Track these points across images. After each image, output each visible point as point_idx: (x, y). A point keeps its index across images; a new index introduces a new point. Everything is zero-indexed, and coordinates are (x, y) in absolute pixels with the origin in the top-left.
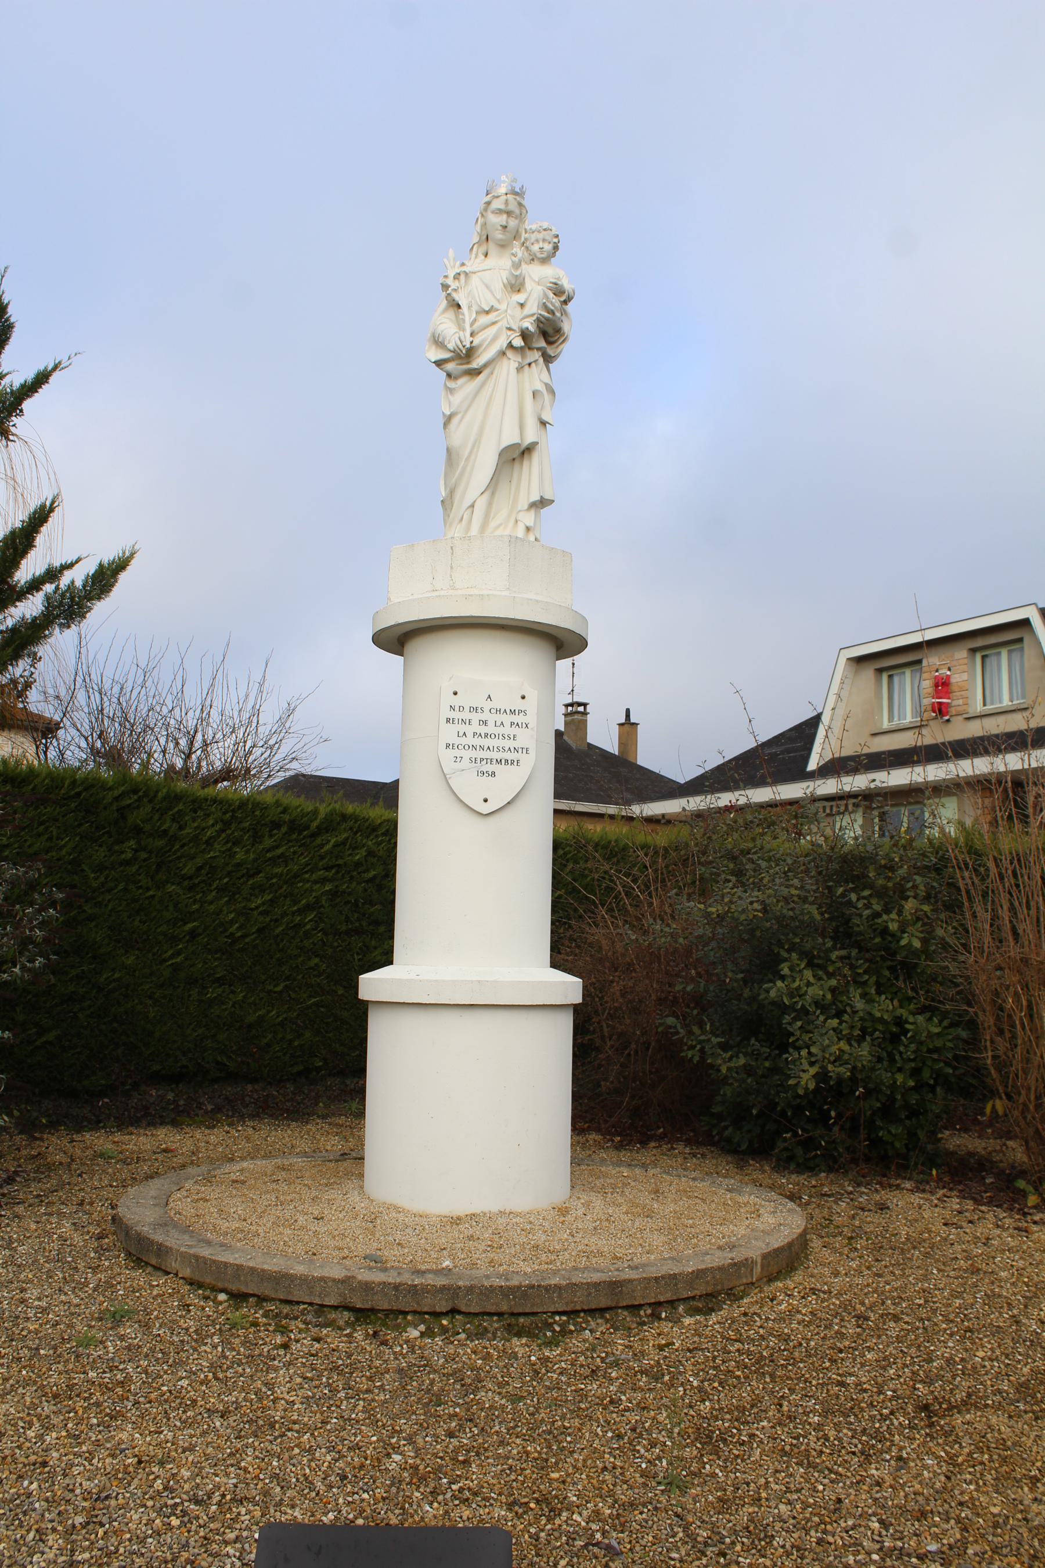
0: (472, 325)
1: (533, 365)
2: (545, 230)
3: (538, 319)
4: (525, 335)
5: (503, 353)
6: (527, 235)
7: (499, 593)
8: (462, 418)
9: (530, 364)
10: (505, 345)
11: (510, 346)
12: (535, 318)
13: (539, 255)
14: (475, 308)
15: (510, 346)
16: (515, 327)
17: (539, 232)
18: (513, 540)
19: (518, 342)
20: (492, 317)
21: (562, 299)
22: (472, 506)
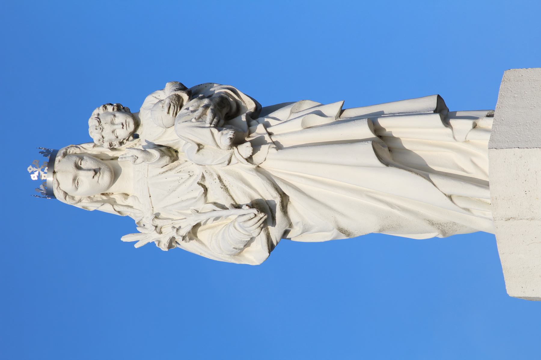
0: (223, 208)
1: (269, 130)
2: (100, 122)
3: (216, 126)
4: (236, 142)
5: (258, 169)
6: (106, 145)
8: (342, 214)
9: (270, 134)
11: (249, 159)
12: (215, 131)
13: (132, 127)
14: (201, 206)
15: (249, 159)
16: (227, 154)
18: (494, 146)
19: (246, 149)
20: (212, 184)
21: (185, 97)
22: (450, 197)
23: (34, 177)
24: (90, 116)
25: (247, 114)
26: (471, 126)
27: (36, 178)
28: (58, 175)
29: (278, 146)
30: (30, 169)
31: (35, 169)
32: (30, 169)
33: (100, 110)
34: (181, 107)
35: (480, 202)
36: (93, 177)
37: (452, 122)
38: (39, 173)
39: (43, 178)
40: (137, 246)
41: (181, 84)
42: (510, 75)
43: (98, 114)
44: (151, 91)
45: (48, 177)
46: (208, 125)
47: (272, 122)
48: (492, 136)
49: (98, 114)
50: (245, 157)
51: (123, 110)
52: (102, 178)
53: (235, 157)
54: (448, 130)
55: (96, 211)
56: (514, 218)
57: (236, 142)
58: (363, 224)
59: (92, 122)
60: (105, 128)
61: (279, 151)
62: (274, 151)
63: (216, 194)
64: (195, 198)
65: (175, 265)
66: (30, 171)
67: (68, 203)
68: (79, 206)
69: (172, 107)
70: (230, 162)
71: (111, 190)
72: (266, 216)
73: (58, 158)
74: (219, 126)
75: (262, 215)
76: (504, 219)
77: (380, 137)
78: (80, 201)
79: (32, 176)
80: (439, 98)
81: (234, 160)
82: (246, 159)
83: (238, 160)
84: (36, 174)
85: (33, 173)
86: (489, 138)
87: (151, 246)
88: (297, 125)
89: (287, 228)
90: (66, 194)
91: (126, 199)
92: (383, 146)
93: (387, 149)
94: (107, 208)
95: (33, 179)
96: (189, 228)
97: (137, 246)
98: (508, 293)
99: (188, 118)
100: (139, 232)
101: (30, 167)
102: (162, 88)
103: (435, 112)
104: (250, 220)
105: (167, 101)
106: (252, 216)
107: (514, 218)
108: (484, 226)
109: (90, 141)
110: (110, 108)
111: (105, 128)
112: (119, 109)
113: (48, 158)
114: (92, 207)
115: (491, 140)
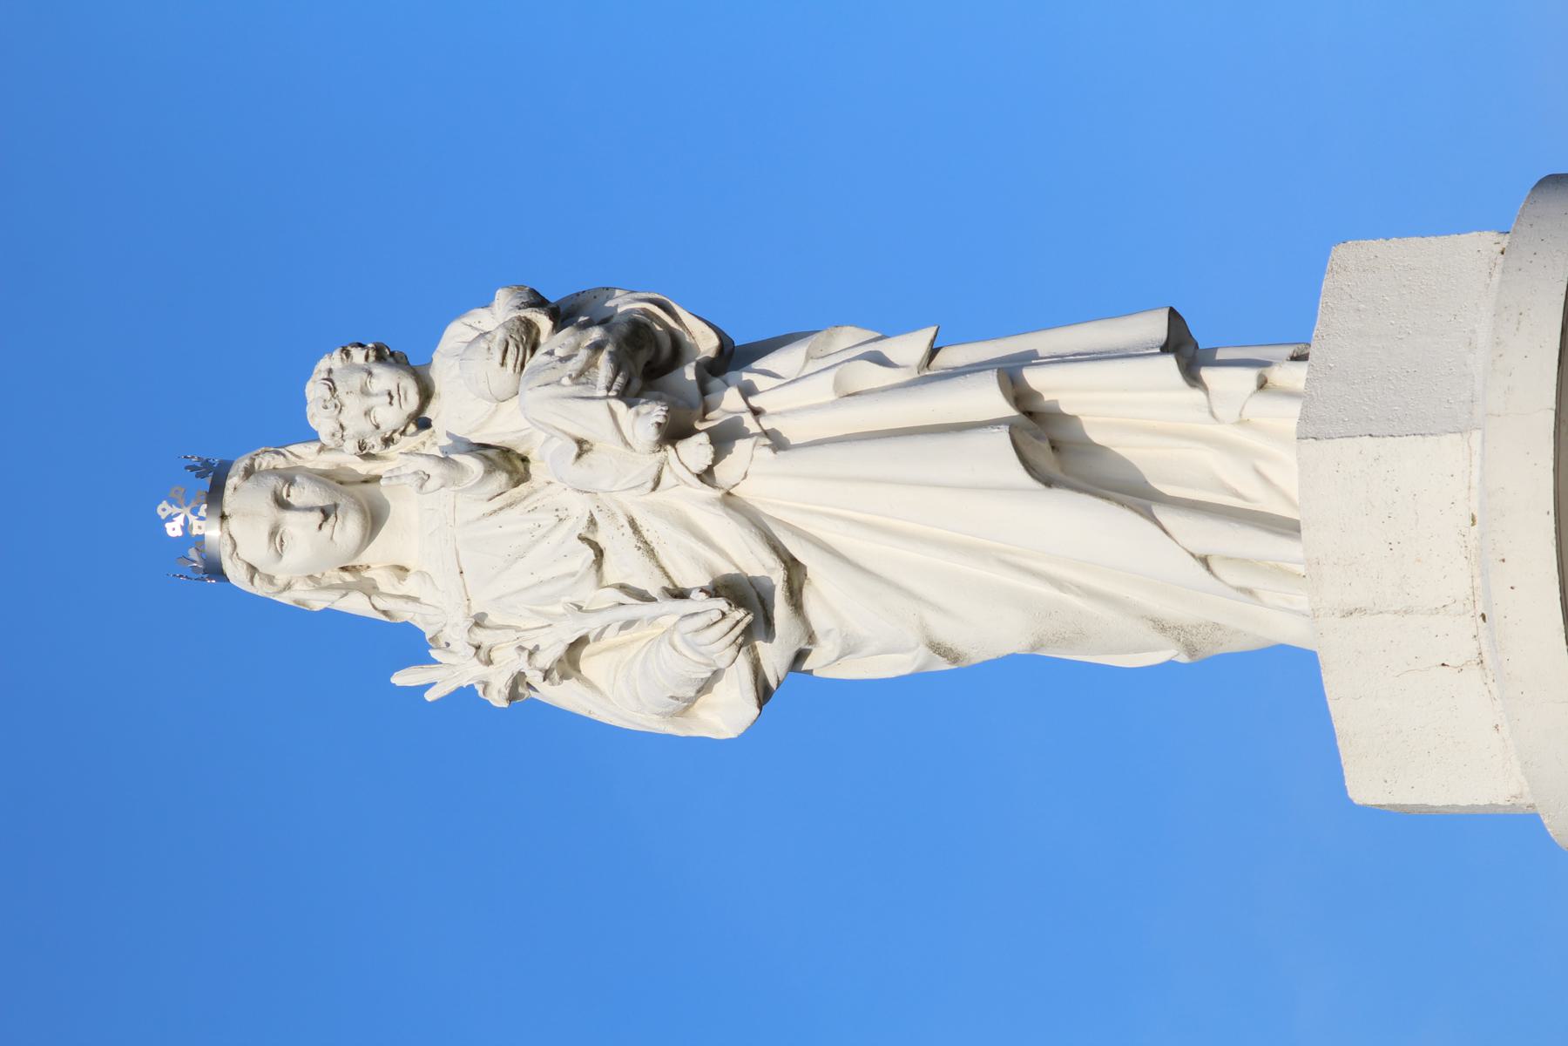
0: (644, 597)
1: (755, 401)
2: (333, 389)
3: (621, 396)
4: (673, 433)
5: (729, 500)
6: (351, 446)
7: (1476, 460)
8: (938, 608)
9: (756, 412)
10: (707, 492)
11: (706, 476)
12: (620, 407)
13: (413, 401)
14: (588, 594)
15: (706, 476)
16: (650, 462)
17: (340, 408)
18: (1310, 431)
19: (696, 450)
20: (612, 537)
21: (544, 322)
22: (1204, 561)
23: (174, 529)
24: (307, 374)
25: (698, 364)
26: (1253, 385)
27: (179, 533)
28: (233, 524)
29: (777, 442)
30: (164, 509)
31: (175, 510)
32: (164, 509)
33: (334, 360)
34: (534, 349)
35: (1278, 572)
37: (1206, 374)
38: (186, 520)
39: (195, 532)
40: (430, 696)
41: (533, 292)
42: (1346, 255)
43: (330, 371)
44: (458, 310)
45: (207, 528)
46: (603, 393)
47: (760, 382)
48: (1304, 407)
49: (330, 371)
50: (697, 470)
51: (391, 360)
52: (343, 528)
54: (1197, 395)
55: (328, 612)
56: (1363, 611)
57: (673, 433)
58: (991, 631)
59: (315, 390)
60: (348, 403)
61: (780, 453)
62: (768, 453)
63: (625, 564)
64: (573, 575)
65: (525, 742)
66: (163, 515)
67: (260, 593)
68: (285, 598)
69: (512, 348)
70: (657, 482)
71: (363, 559)
72: (750, 617)
73: (232, 481)
74: (629, 395)
75: (739, 614)
76: (1338, 614)
77: (1029, 414)
78: (288, 586)
79: (169, 526)
80: (1173, 313)
81: (666, 478)
82: (699, 476)
83: (677, 477)
85: (170, 518)
87: (465, 695)
88: (821, 388)
89: (803, 645)
90: (253, 569)
91: (401, 579)
92: (1038, 437)
93: (1048, 444)
94: (356, 604)
95: (171, 533)
96: (560, 650)
97: (430, 696)
98: (1351, 795)
100: (436, 662)
101: (164, 504)
102: (486, 303)
103: (1165, 349)
104: (709, 626)
105: (500, 335)
106: (716, 616)
107: (1363, 611)
108: (1290, 631)
109: (311, 436)
110: (358, 355)
111: (348, 403)
112: (381, 357)
113: (208, 480)
114: (318, 601)
115: (1304, 418)
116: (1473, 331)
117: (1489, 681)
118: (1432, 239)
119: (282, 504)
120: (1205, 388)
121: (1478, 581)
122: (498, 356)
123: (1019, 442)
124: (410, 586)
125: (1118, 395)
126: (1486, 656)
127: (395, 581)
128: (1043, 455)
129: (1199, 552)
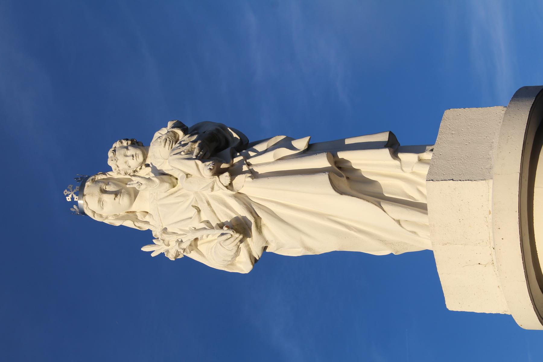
4: (218, 172)
11: (230, 186)
12: (199, 162)
13: (141, 159)
19: (225, 178)
20: (203, 207)
21: (180, 133)
22: (398, 222)
23: (69, 199)
26: (416, 160)
28: (87, 198)
29: (254, 175)
30: (66, 192)
31: (69, 193)
36: (115, 199)
37: (400, 155)
38: (72, 196)
39: (75, 200)
40: (153, 255)
41: (181, 123)
44: (159, 129)
45: (79, 199)
47: (252, 154)
48: (430, 169)
51: (136, 144)
53: (217, 185)
54: (397, 162)
55: (121, 226)
58: (323, 244)
59: (110, 154)
62: (250, 179)
66: (65, 194)
68: (106, 221)
70: (213, 189)
71: (132, 209)
73: (88, 183)
74: (203, 158)
75: (237, 235)
78: (107, 218)
79: (67, 198)
80: (391, 135)
81: (215, 189)
82: (226, 187)
83: (219, 187)
84: (70, 196)
85: (68, 195)
86: (426, 173)
88: (269, 157)
89: (264, 245)
90: (94, 212)
92: (341, 176)
93: (345, 179)
94: (129, 224)
95: (68, 200)
99: (179, 151)
100: (154, 244)
101: (66, 191)
104: (227, 239)
110: (125, 143)
114: (117, 223)
115: (429, 173)
116: (493, 142)
117: (496, 270)
118: (480, 108)
119: (104, 191)
120: (399, 160)
121: (491, 234)
122: (163, 144)
123: (331, 177)
124: (147, 218)
125: (371, 163)
126: (495, 262)
127: (143, 217)
128: (343, 183)
129: (397, 218)
